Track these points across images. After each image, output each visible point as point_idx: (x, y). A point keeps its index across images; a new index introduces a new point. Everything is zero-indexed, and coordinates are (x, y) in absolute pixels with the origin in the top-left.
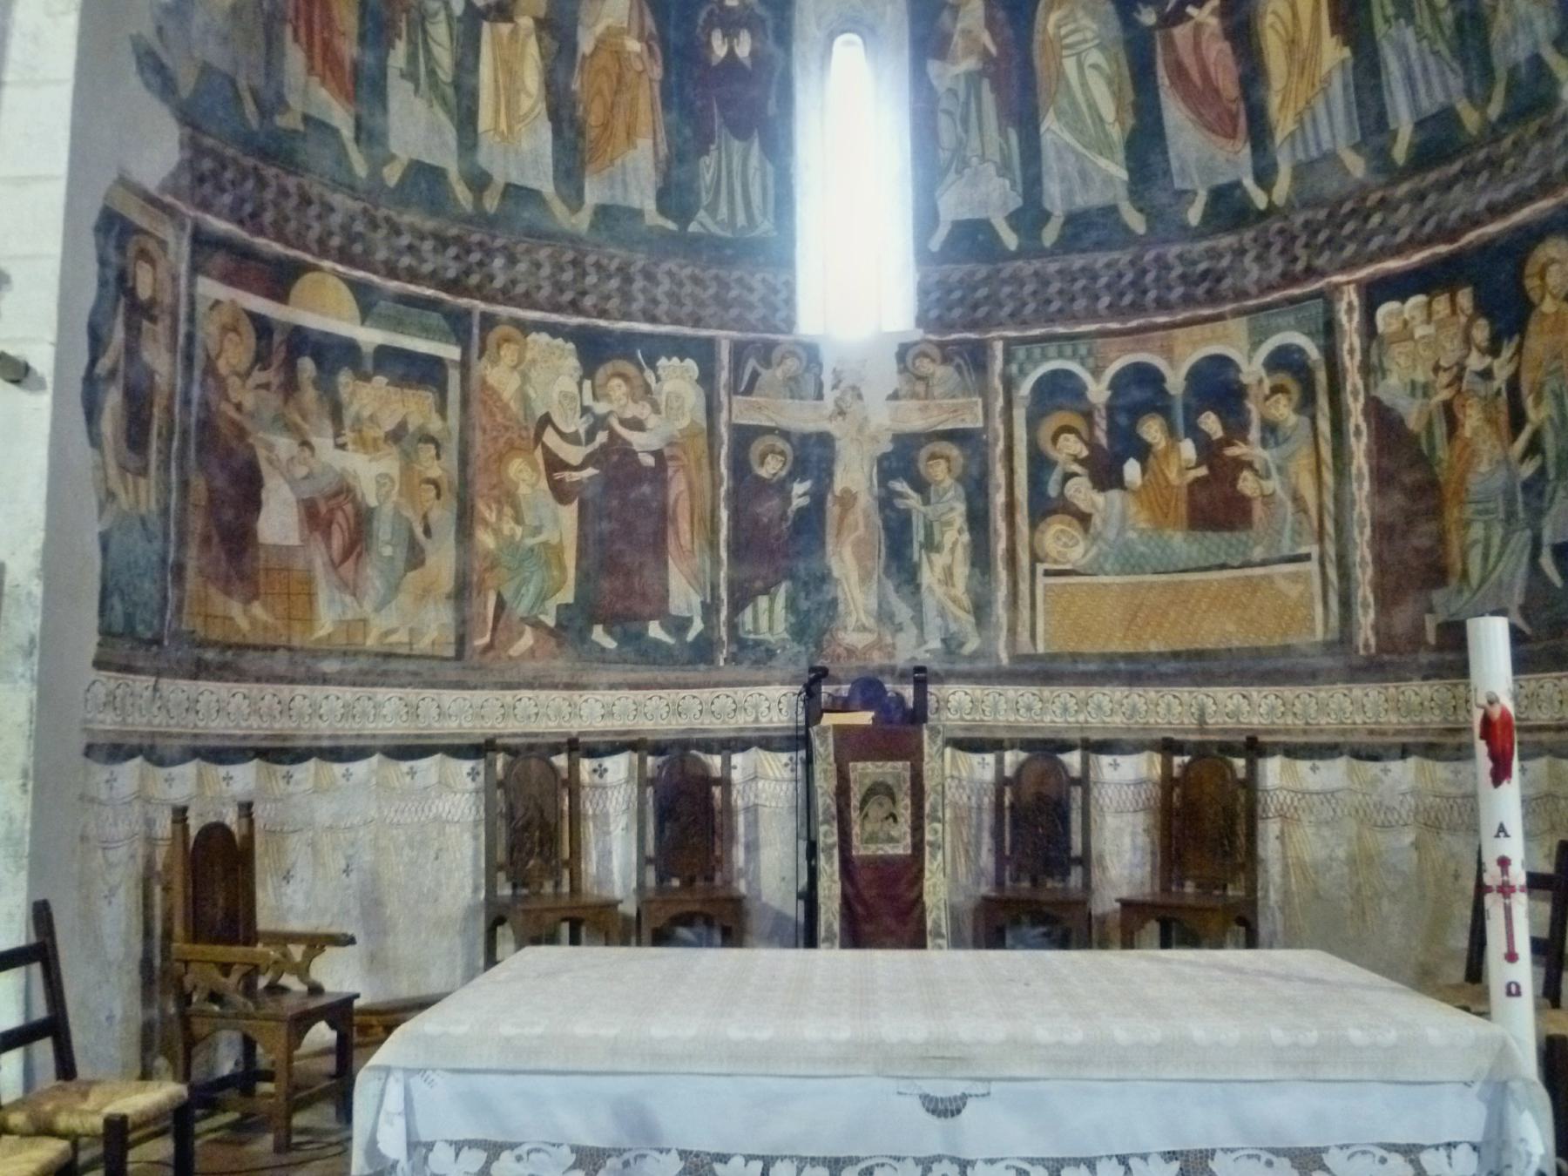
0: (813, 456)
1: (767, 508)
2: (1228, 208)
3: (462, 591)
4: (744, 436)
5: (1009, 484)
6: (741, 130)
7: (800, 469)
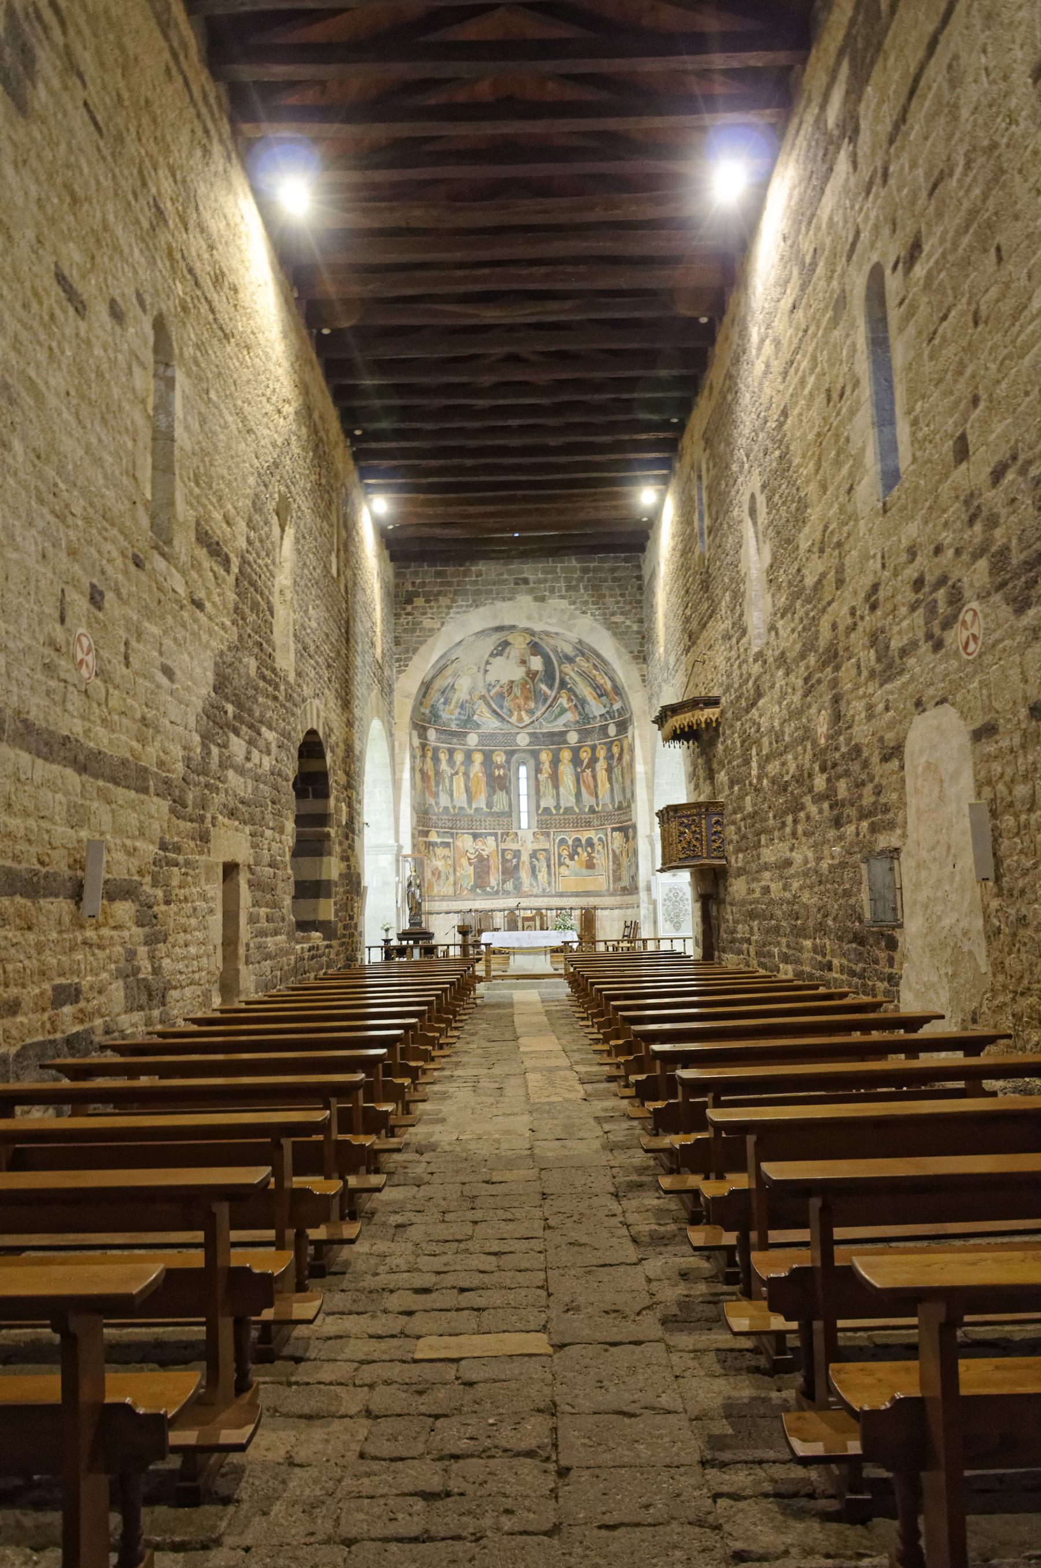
0: (517, 854)
1: (508, 865)
2: (592, 810)
3: (455, 884)
4: (504, 851)
5: (554, 860)
6: (501, 789)
7: (514, 857)
